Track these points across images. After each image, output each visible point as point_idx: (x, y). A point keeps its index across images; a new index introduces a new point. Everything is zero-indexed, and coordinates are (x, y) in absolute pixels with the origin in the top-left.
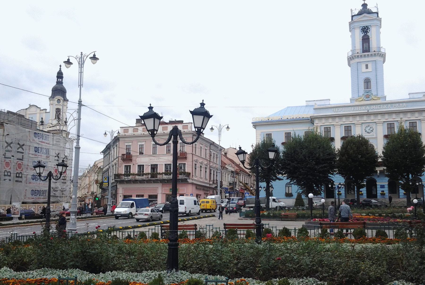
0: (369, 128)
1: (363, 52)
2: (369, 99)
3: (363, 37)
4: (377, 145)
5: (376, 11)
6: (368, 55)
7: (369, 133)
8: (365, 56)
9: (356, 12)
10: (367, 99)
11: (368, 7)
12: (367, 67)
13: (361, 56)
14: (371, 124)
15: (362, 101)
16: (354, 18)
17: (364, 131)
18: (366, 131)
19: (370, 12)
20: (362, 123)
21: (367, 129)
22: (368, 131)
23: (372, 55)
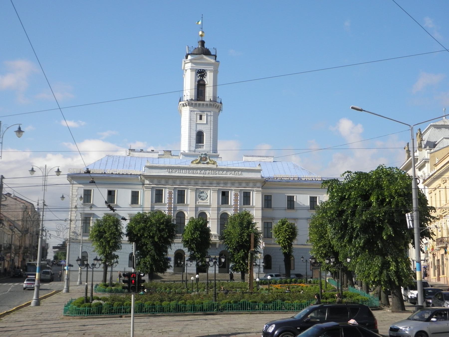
1: (197, 100)
2: (205, 162)
3: (199, 81)
5: (214, 54)
6: (203, 104)
8: (200, 104)
9: (192, 50)
11: (206, 46)
12: (201, 118)
13: (196, 104)
14: (205, 191)
16: (189, 57)
19: (207, 53)
23: (207, 105)
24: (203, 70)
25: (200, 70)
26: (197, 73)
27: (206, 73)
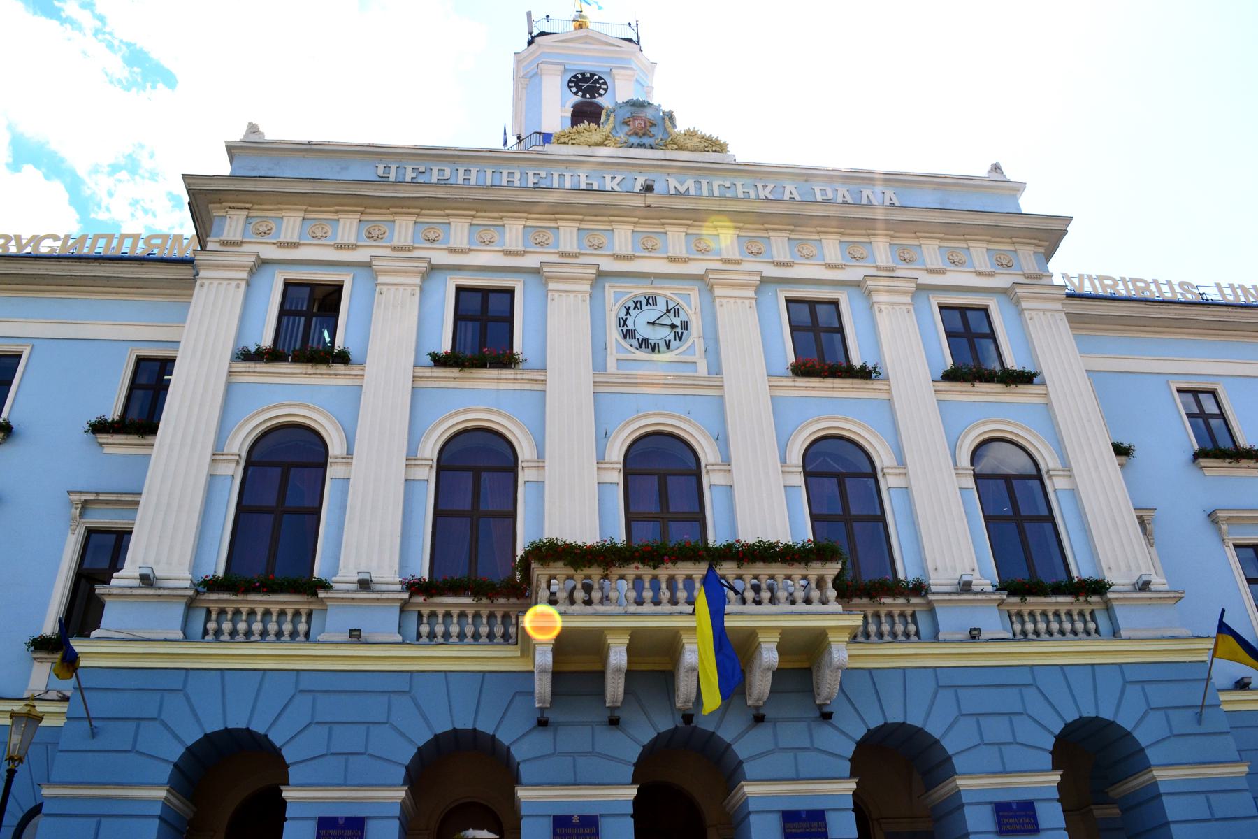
0: (651, 313)
2: (646, 140)
4: (722, 440)
5: (635, 39)
7: (654, 348)
10: (635, 140)
14: (665, 292)
15: (601, 144)
17: (614, 334)
18: (629, 334)
20: (602, 275)
21: (640, 322)
22: (644, 331)
24: (592, 75)
25: (583, 74)
26: (570, 81)
27: (605, 83)
